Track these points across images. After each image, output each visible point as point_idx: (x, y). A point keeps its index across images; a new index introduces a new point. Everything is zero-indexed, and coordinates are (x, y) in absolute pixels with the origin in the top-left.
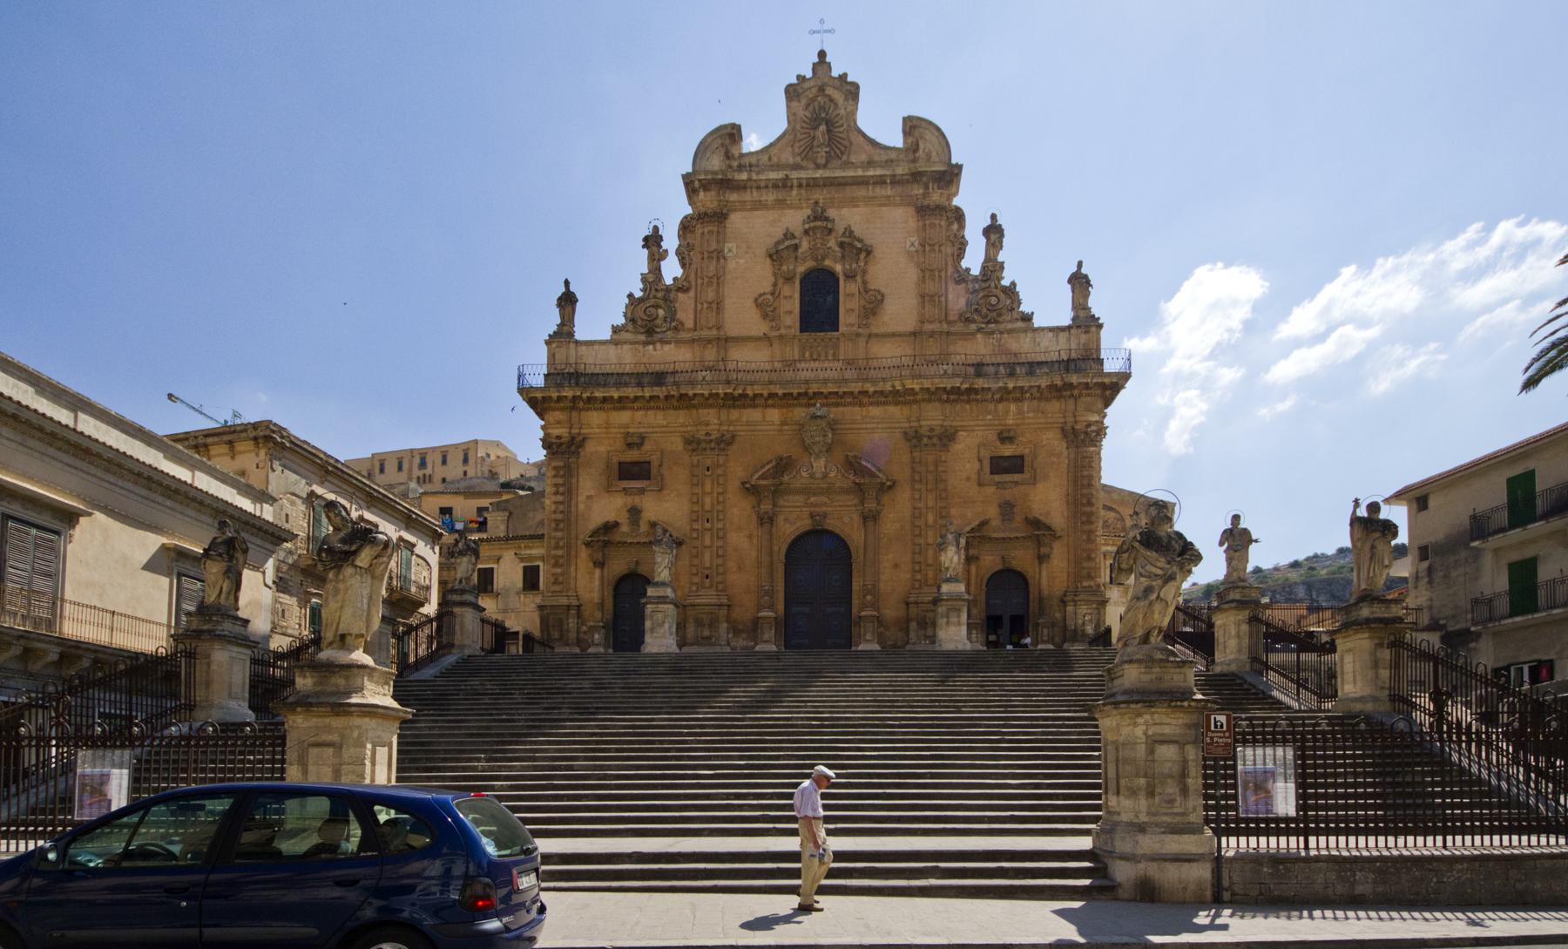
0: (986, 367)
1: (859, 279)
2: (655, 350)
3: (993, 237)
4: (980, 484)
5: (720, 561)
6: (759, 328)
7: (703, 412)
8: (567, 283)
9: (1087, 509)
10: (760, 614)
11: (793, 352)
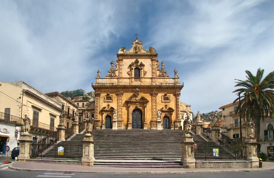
1: (143, 69)
4: (162, 102)
6: (128, 76)
7: (119, 89)
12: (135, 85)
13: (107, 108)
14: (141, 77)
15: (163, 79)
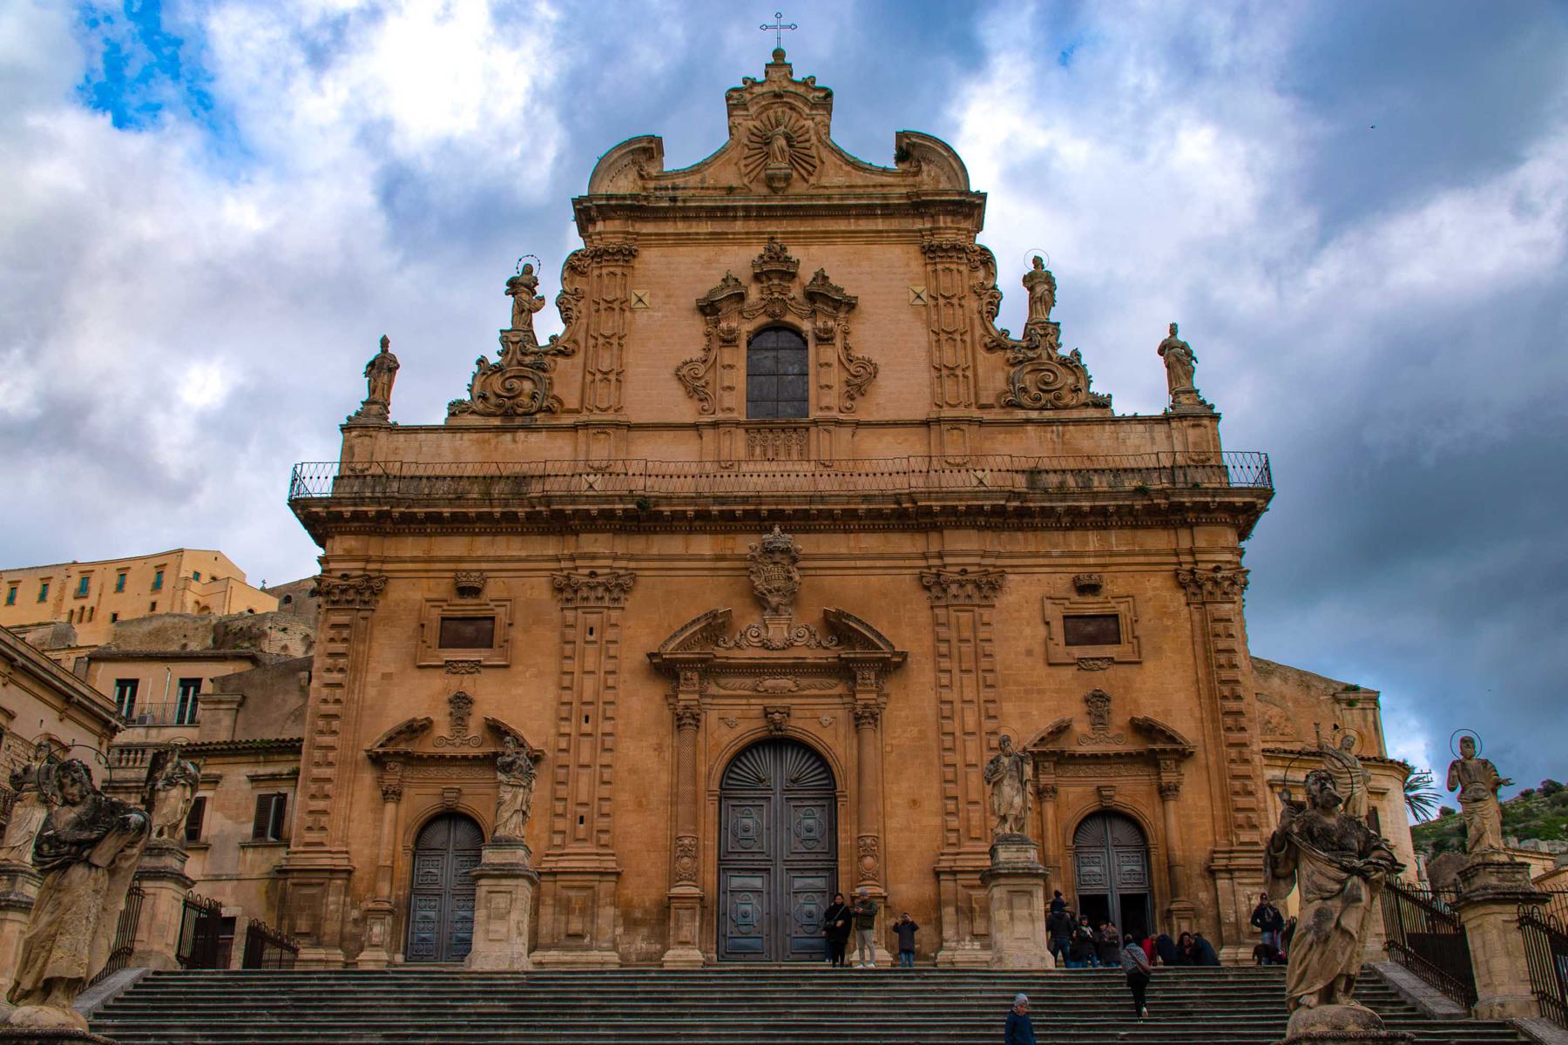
0: (1044, 475)
1: (838, 342)
2: (514, 441)
3: (1041, 289)
5: (605, 791)
6: (686, 411)
8: (385, 343)
9: (1232, 705)
10: (675, 891)
11: (738, 444)
12: (759, 498)
13: (443, 729)
14: (814, 414)
15: (1050, 434)
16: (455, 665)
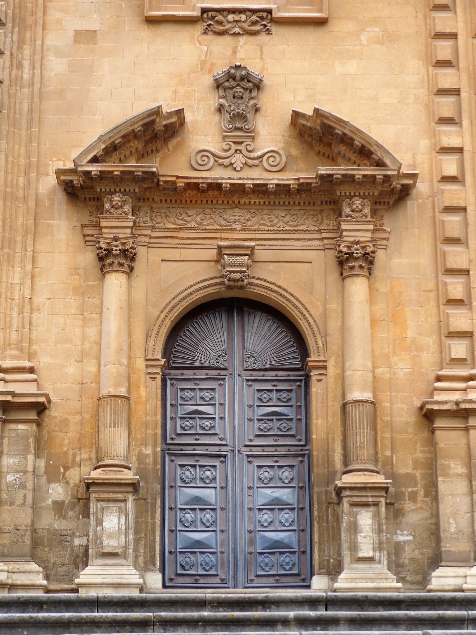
16: (220, 17)
